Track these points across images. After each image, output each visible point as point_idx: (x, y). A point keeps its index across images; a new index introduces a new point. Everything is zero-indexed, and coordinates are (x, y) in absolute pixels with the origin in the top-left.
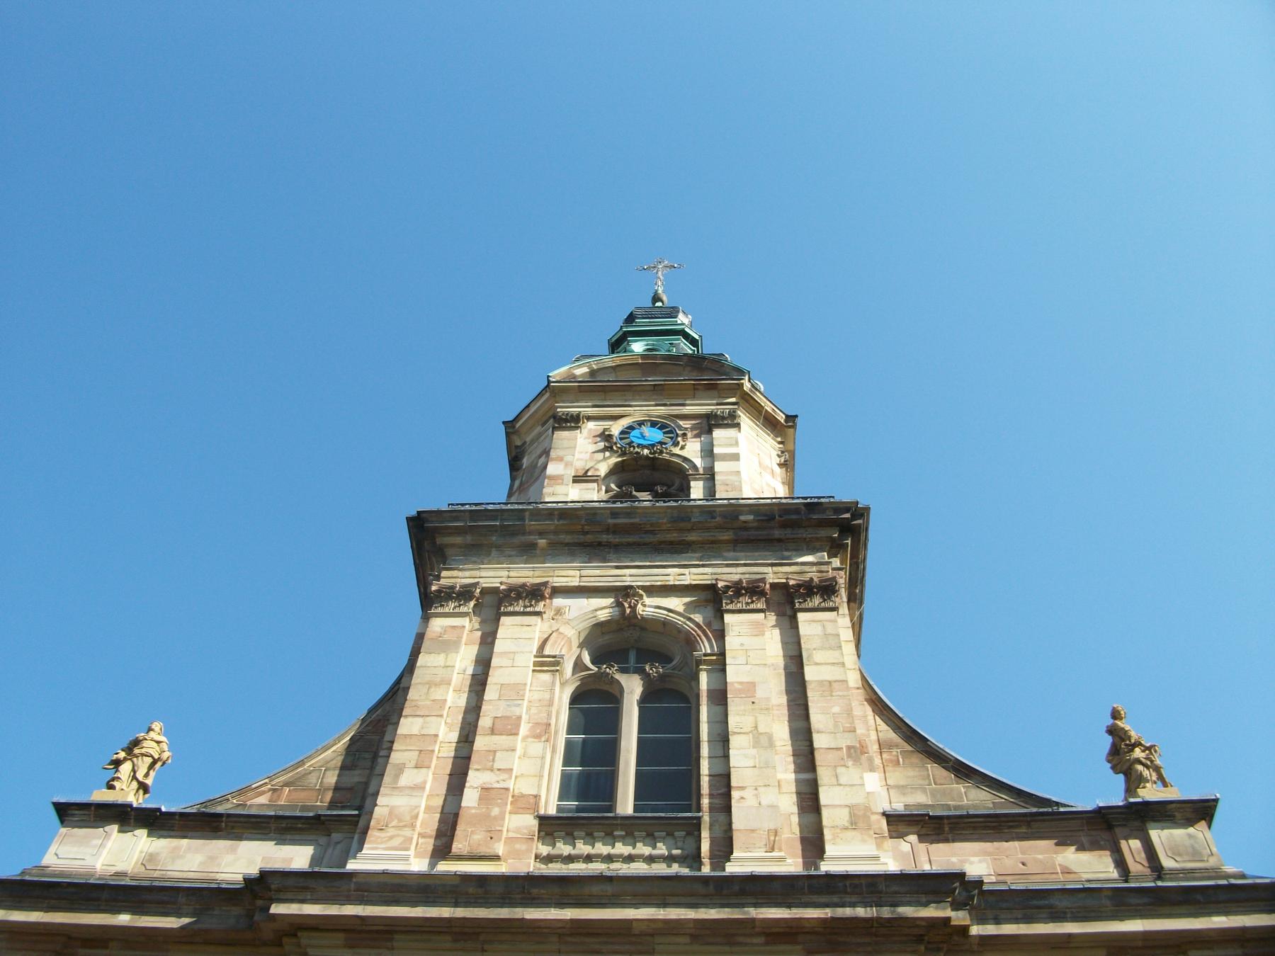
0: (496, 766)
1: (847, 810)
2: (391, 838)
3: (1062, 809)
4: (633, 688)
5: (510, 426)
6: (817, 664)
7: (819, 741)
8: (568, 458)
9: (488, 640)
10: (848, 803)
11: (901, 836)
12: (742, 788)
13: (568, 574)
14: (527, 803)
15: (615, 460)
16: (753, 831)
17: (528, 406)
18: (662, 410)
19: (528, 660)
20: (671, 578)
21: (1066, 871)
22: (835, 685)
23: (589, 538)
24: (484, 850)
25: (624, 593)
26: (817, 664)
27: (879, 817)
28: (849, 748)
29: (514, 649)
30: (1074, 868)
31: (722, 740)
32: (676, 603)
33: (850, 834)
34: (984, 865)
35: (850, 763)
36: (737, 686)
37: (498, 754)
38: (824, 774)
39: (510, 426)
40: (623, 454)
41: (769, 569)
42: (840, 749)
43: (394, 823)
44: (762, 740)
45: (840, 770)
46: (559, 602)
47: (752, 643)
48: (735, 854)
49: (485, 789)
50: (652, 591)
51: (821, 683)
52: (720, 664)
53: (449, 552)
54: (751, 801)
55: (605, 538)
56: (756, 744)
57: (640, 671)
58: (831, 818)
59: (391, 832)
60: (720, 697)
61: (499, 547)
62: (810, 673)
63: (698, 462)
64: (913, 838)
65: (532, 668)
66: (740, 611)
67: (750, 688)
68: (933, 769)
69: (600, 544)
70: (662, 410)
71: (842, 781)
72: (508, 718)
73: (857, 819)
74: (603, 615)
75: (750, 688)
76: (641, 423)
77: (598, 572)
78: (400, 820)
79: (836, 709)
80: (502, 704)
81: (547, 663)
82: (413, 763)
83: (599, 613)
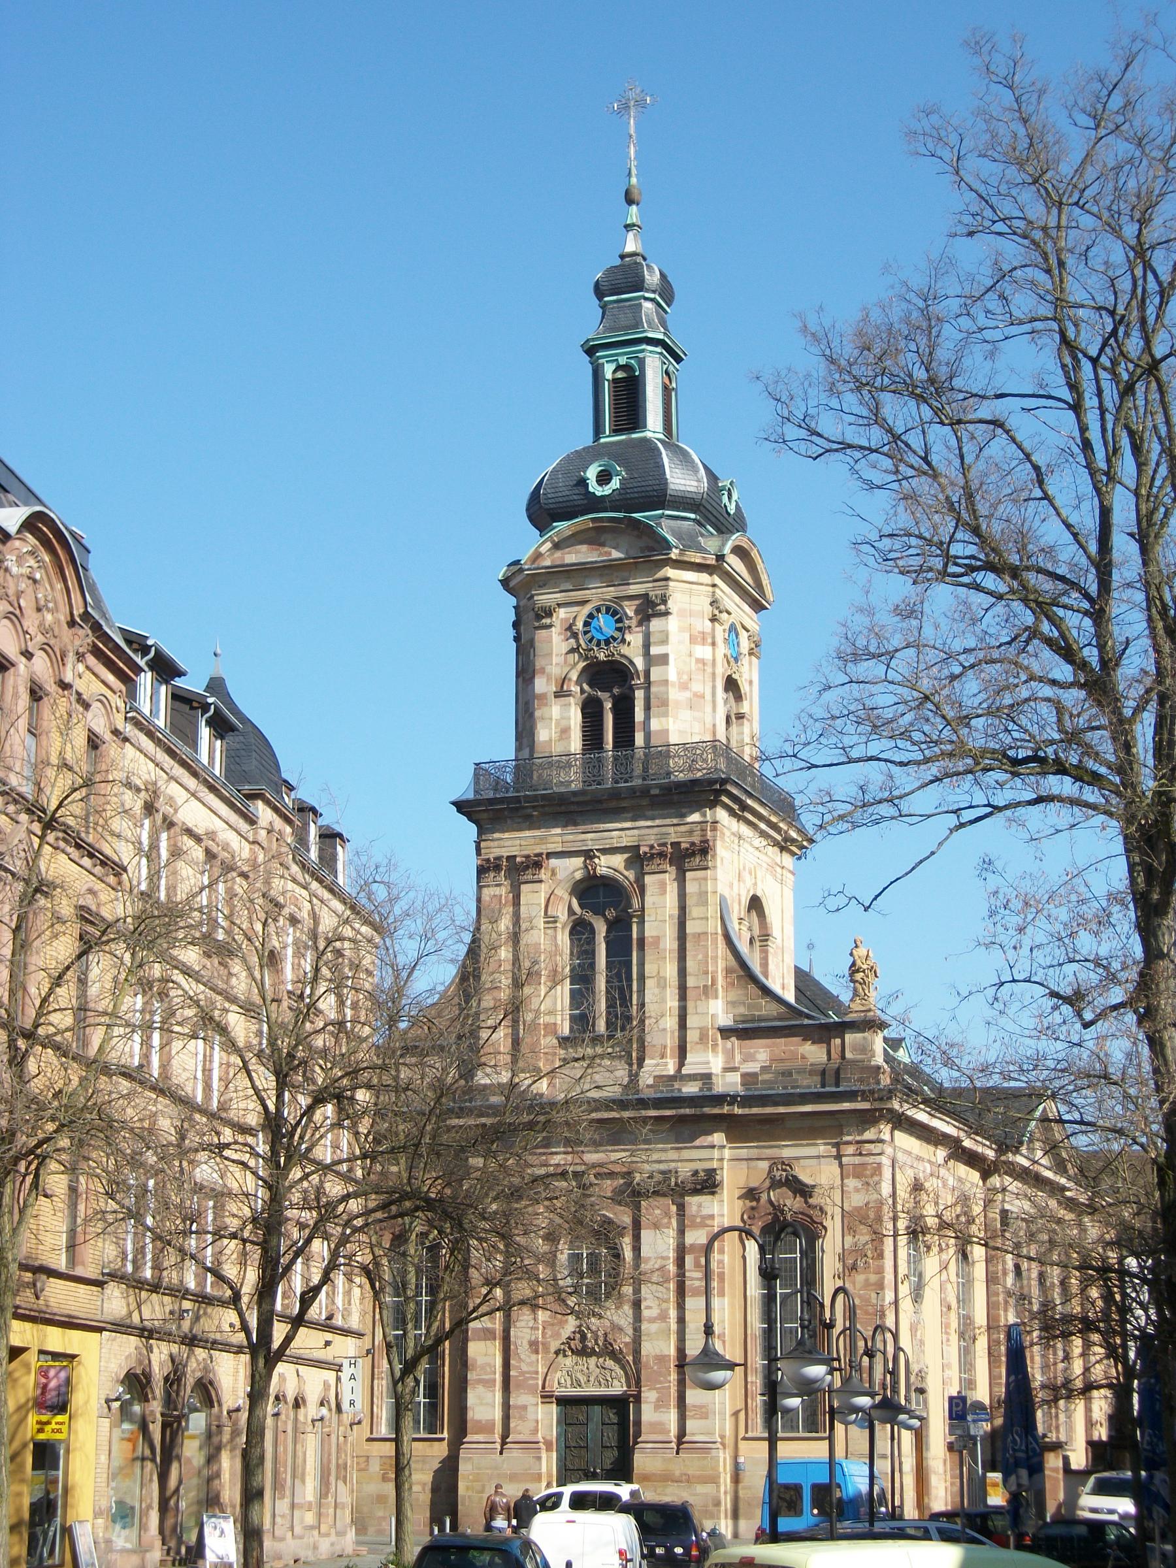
3: (806, 1022)
4: (601, 928)
7: (691, 982)
8: (548, 669)
9: (516, 902)
11: (728, 1038)
13: (556, 837)
14: (551, 1029)
15: (582, 664)
18: (612, 592)
19: (540, 922)
21: (803, 1057)
23: (563, 808)
25: (588, 855)
31: (642, 978)
32: (618, 861)
38: (690, 1005)
40: (587, 658)
41: (671, 830)
44: (662, 983)
46: (553, 862)
47: (659, 899)
50: (605, 851)
51: (694, 935)
52: (642, 922)
55: (573, 808)
56: (659, 985)
57: (604, 916)
58: (692, 1036)
60: (641, 941)
62: (691, 928)
63: (639, 663)
64: (733, 1039)
65: (542, 925)
67: (657, 939)
68: (751, 987)
70: (612, 592)
73: (703, 1038)
74: (579, 875)
75: (657, 939)
76: (598, 610)
77: (571, 837)
81: (551, 921)
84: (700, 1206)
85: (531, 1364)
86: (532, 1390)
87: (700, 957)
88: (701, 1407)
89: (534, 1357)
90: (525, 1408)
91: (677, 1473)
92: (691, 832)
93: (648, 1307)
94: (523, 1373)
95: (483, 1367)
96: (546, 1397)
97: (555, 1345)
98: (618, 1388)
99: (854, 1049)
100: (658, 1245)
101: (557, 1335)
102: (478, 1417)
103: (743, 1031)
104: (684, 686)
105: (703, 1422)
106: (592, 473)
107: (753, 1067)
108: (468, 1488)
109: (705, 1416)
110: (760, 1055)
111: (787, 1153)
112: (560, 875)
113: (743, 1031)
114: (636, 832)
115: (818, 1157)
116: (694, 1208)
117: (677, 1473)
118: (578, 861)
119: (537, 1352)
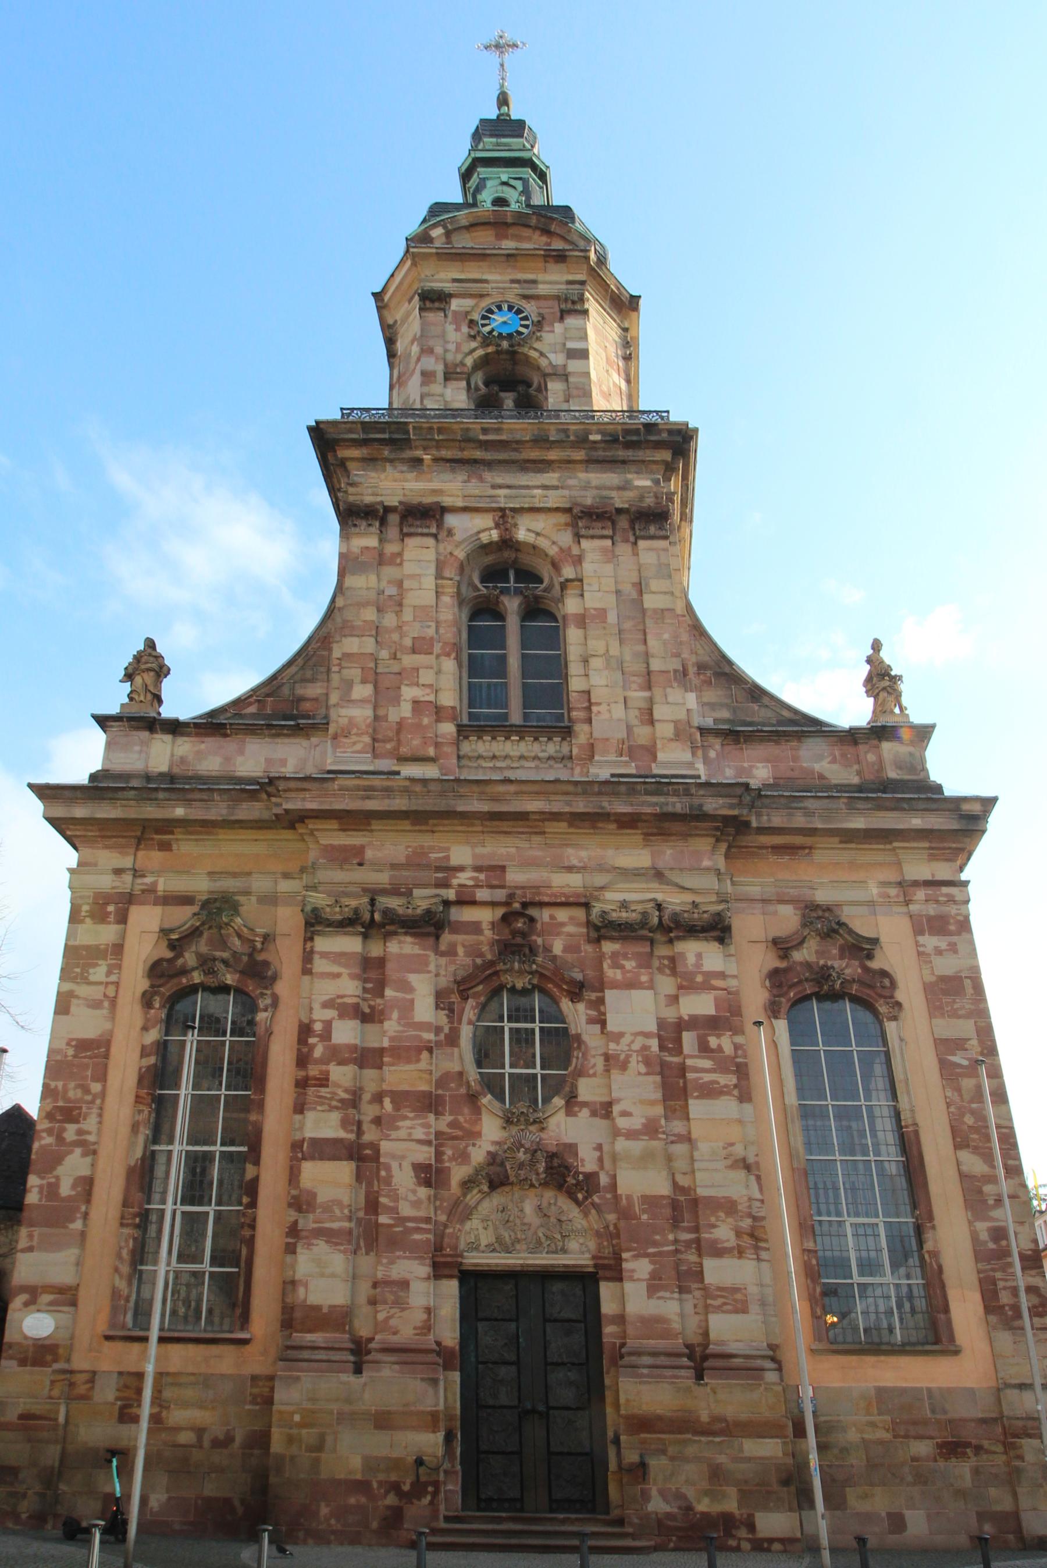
0: (421, 682)
1: (672, 725)
2: (354, 743)
5: (377, 296)
6: (654, 593)
10: (674, 718)
12: (599, 704)
16: (607, 740)
17: (392, 275)
20: (536, 500)
22: (666, 613)
24: (421, 753)
26: (654, 593)
27: (693, 730)
28: (675, 671)
29: (418, 571)
30: (827, 774)
33: (674, 744)
34: (766, 770)
35: (675, 685)
36: (593, 612)
37: (421, 671)
39: (377, 296)
42: (668, 672)
43: (355, 731)
45: (669, 690)
48: (597, 758)
49: (416, 703)
51: (655, 611)
53: (350, 465)
54: (605, 716)
59: (354, 738)
61: (391, 461)
66: (593, 537)
69: (475, 461)
71: (670, 699)
72: (424, 638)
78: (358, 729)
79: (666, 636)
80: (417, 625)
82: (358, 679)
83: (481, 535)
84: (699, 956)
85: (416, 1204)
86: (414, 1250)
87: (666, 636)
88: (735, 1290)
89: (423, 1192)
90: (405, 1284)
91: (705, 1417)
92: (642, 498)
93: (625, 1114)
94: (402, 1220)
95: (327, 1208)
96: (443, 1266)
97: (458, 1173)
98: (578, 1254)
99: (899, 766)
100: (635, 1011)
101: (463, 1157)
102: (313, 1299)
105: (740, 1317)
108: (290, 1440)
109: (742, 1308)
111: (822, 896)
112: (458, 537)
113: (734, 735)
114: (566, 492)
115: (871, 904)
116: (691, 959)
117: (705, 1417)
119: (428, 1183)
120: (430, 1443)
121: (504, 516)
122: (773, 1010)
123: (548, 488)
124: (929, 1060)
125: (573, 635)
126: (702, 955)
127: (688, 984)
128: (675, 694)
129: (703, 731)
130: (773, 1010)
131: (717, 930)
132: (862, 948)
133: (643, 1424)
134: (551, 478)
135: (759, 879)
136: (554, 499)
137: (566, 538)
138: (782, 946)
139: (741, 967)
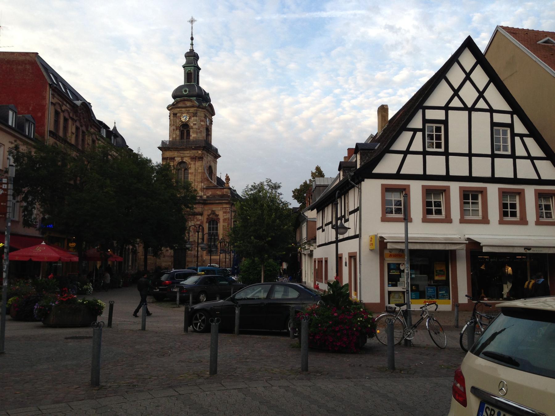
103: (208, 188)
104: (199, 129)
106: (183, 90)
107: (208, 195)
110: (210, 193)
111: (214, 209)
113: (208, 188)
118: (180, 159)
120: (170, 263)
121: (182, 158)
122: (207, 222)
123: (187, 153)
124: (221, 227)
125: (190, 175)
126: (199, 217)
127: (198, 220)
128: (200, 184)
129: (204, 188)
130: (207, 222)
131: (201, 214)
132: (217, 215)
133: (188, 262)
134: (188, 152)
135: (206, 208)
136: (188, 155)
137: (190, 161)
138: (209, 215)
139: (204, 218)
